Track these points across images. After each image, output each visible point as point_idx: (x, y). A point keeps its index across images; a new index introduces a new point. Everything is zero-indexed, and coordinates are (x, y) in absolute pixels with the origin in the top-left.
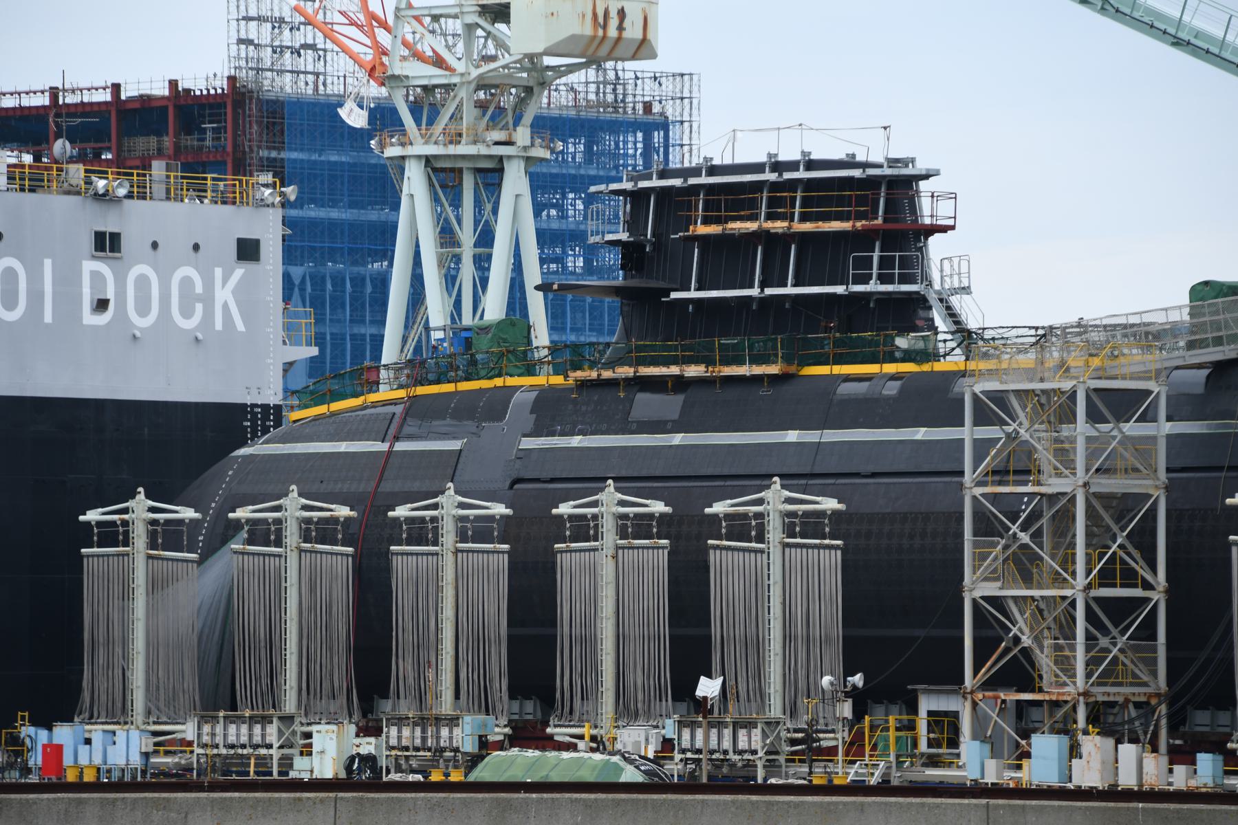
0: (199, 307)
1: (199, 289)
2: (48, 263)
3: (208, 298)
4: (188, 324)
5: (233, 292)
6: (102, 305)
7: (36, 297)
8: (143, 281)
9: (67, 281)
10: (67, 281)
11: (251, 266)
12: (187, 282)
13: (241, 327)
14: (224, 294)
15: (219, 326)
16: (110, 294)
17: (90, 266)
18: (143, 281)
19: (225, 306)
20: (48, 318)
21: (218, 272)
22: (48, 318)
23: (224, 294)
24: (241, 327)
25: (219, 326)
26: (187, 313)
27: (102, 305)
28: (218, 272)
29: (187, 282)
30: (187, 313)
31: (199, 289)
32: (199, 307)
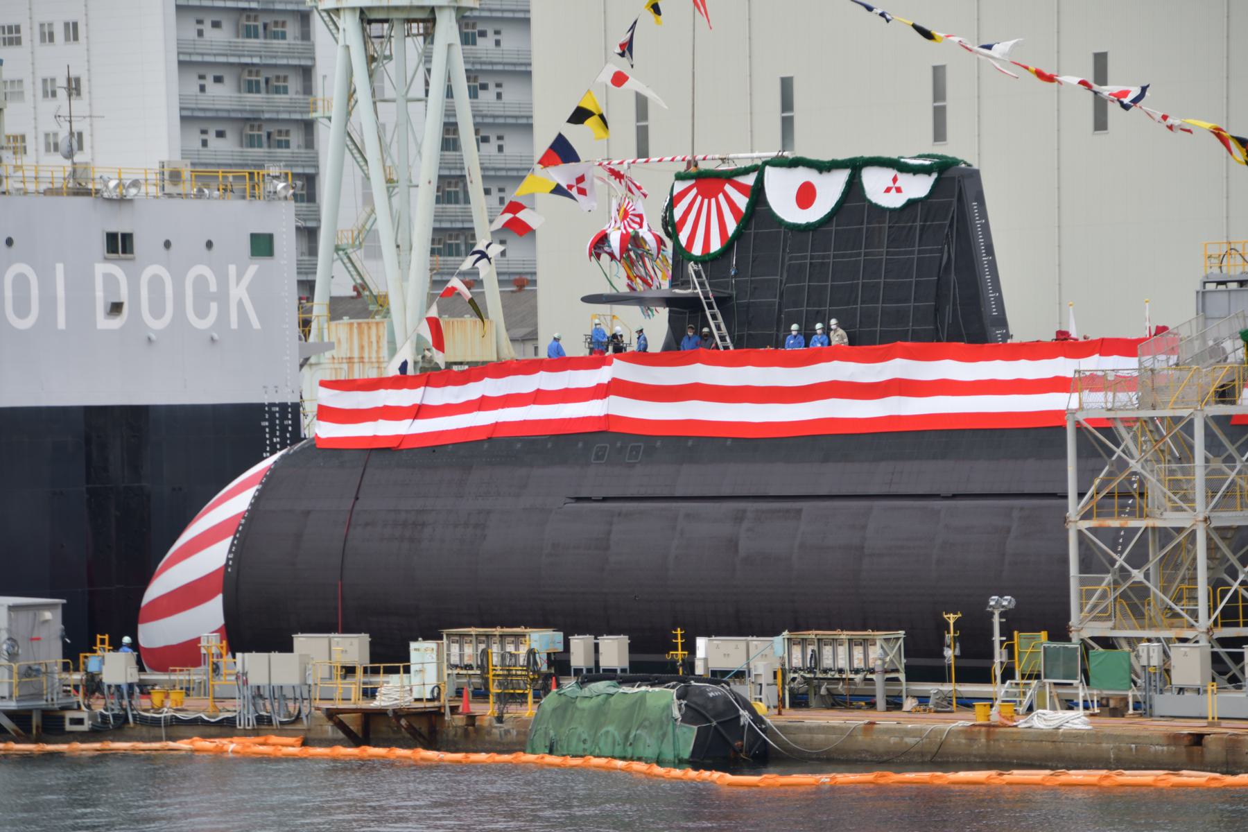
0: (214, 307)
1: (213, 288)
2: (60, 268)
3: (222, 297)
4: (202, 324)
5: (249, 289)
6: (116, 308)
7: (48, 302)
8: (156, 282)
9: (80, 285)
10: (80, 285)
11: (265, 261)
12: (201, 281)
13: (256, 324)
14: (238, 292)
15: (234, 325)
16: (124, 297)
18: (156, 282)
19: (240, 304)
20: (61, 324)
21: (232, 269)
22: (61, 324)
23: (238, 292)
24: (256, 324)
25: (234, 325)
26: (202, 313)
27: (116, 308)
28: (232, 269)
29: (201, 281)
30: (202, 313)
31: (213, 288)
32: (214, 307)
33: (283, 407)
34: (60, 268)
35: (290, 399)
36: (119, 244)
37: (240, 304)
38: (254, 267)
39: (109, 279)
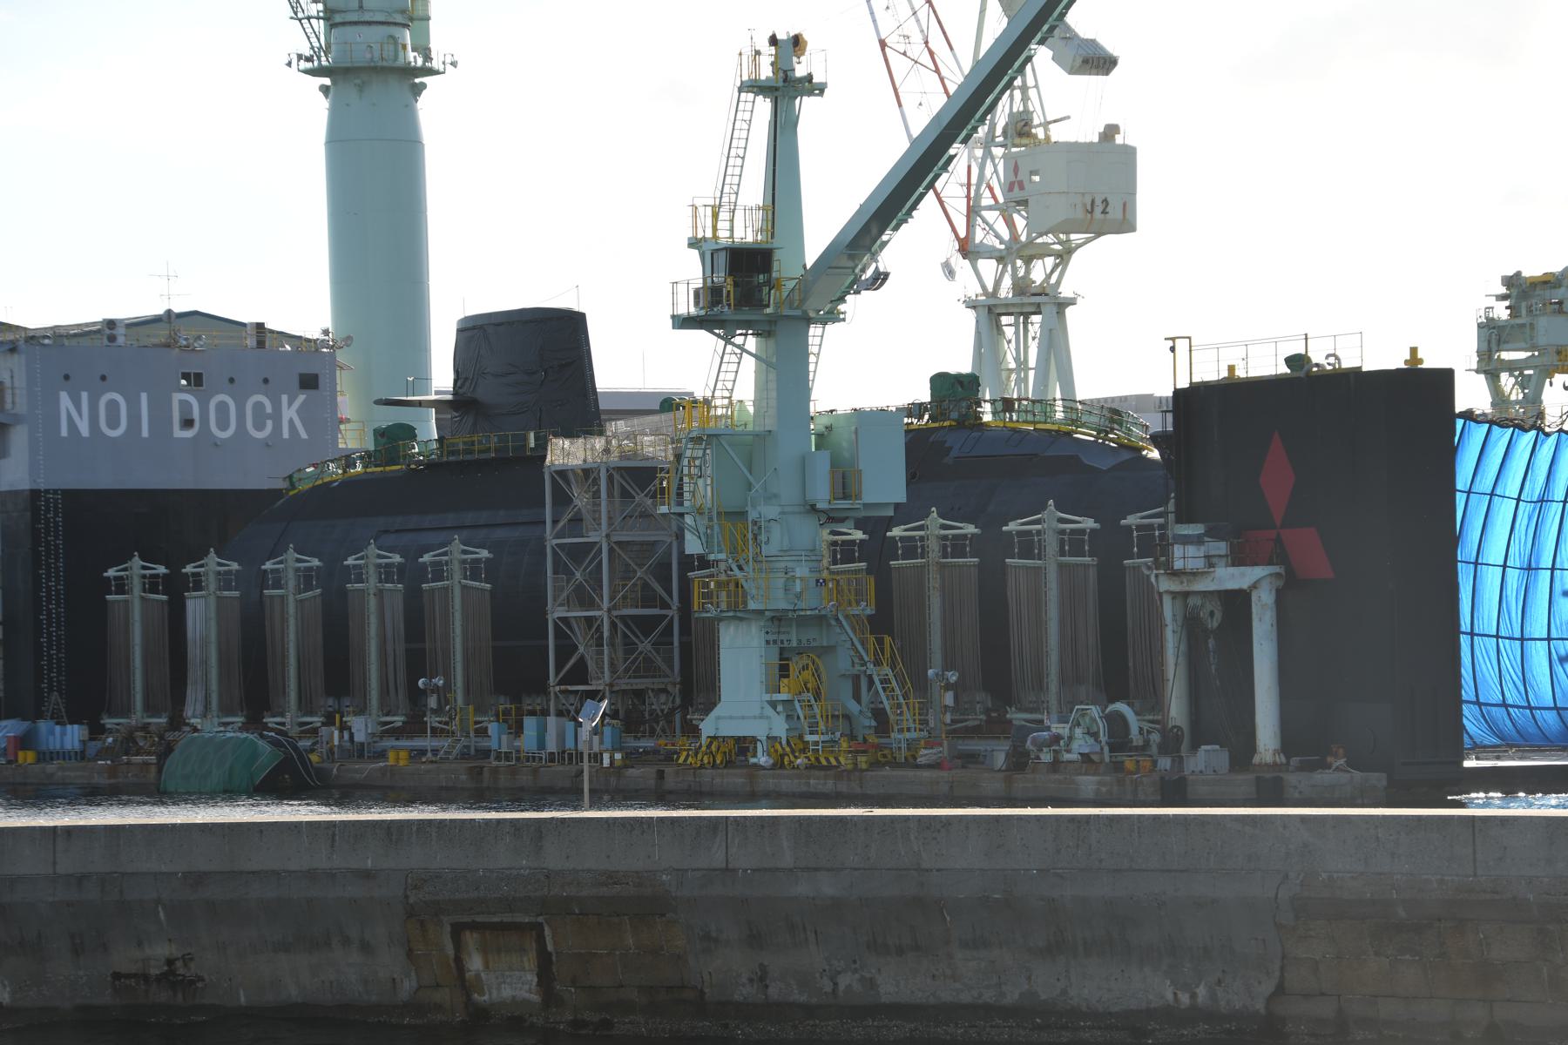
0: (269, 423)
1: (269, 410)
2: (144, 396)
3: (277, 416)
6: (188, 423)
7: (134, 419)
8: (222, 407)
11: (312, 392)
12: (259, 406)
13: (304, 435)
14: (290, 413)
15: (286, 435)
16: (196, 415)
18: (222, 407)
19: (291, 421)
20: (145, 433)
21: (285, 398)
22: (145, 433)
23: (290, 413)
24: (304, 435)
25: (286, 435)
26: (259, 426)
28: (285, 398)
29: (259, 406)
30: (259, 426)
31: (269, 410)
32: (269, 423)
34: (144, 396)
37: (291, 421)
38: (302, 398)
39: (185, 405)
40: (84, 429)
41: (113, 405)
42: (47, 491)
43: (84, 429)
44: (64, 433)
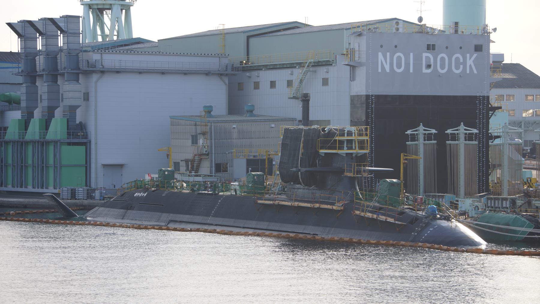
2: (411, 54)
5: (473, 61)
6: (429, 66)
7: (407, 65)
8: (443, 59)
9: (417, 59)
10: (417, 59)
12: (457, 59)
13: (475, 72)
14: (470, 62)
15: (468, 72)
17: (425, 55)
18: (443, 59)
19: (470, 66)
20: (411, 71)
22: (411, 71)
23: (470, 62)
24: (475, 72)
25: (468, 72)
26: (457, 68)
27: (429, 66)
29: (457, 59)
33: (484, 97)
34: (411, 54)
35: (486, 95)
36: (430, 48)
37: (470, 66)
38: (475, 55)
40: (388, 70)
41: (399, 58)
42: (372, 96)
43: (388, 69)
44: (380, 70)
